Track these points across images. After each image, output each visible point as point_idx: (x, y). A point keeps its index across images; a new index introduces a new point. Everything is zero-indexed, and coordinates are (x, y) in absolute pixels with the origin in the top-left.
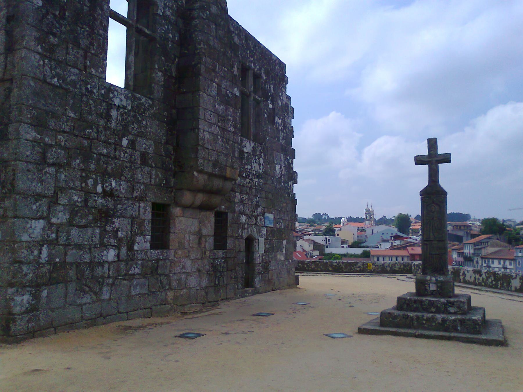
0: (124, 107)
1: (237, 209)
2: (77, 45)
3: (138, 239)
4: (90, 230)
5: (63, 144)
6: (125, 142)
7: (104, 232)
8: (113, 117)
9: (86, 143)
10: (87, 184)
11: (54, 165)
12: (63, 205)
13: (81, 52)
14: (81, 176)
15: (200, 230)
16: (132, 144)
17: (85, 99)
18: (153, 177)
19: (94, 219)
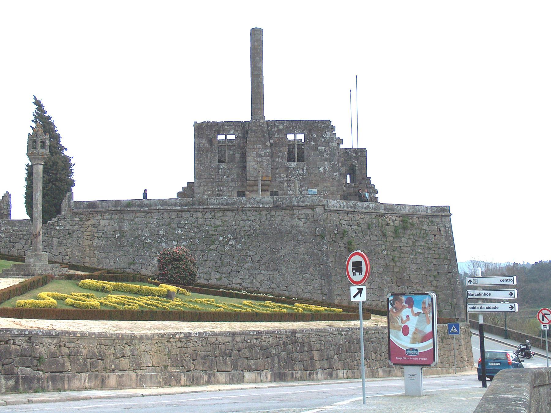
1: (285, 189)
6: (225, 177)
16: (227, 177)
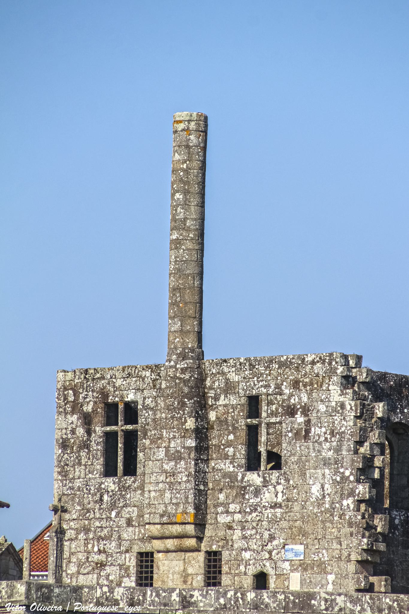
0: (112, 491)
2: (80, 464)
3: (125, 580)
4: (90, 576)
5: (73, 527)
6: (113, 514)
7: (99, 576)
8: (105, 501)
9: (87, 522)
10: (88, 548)
11: (69, 540)
12: (74, 562)
13: (83, 467)
14: (85, 543)
15: (185, 570)
17: (86, 496)
18: (137, 533)
19: (93, 568)
